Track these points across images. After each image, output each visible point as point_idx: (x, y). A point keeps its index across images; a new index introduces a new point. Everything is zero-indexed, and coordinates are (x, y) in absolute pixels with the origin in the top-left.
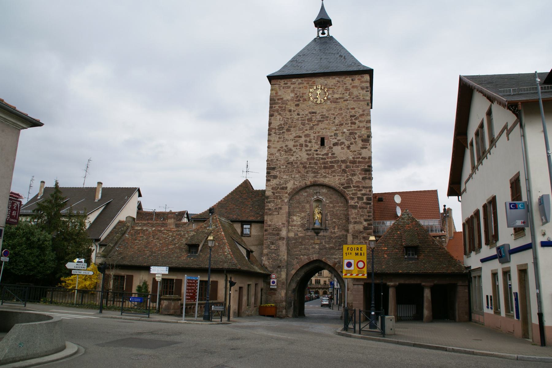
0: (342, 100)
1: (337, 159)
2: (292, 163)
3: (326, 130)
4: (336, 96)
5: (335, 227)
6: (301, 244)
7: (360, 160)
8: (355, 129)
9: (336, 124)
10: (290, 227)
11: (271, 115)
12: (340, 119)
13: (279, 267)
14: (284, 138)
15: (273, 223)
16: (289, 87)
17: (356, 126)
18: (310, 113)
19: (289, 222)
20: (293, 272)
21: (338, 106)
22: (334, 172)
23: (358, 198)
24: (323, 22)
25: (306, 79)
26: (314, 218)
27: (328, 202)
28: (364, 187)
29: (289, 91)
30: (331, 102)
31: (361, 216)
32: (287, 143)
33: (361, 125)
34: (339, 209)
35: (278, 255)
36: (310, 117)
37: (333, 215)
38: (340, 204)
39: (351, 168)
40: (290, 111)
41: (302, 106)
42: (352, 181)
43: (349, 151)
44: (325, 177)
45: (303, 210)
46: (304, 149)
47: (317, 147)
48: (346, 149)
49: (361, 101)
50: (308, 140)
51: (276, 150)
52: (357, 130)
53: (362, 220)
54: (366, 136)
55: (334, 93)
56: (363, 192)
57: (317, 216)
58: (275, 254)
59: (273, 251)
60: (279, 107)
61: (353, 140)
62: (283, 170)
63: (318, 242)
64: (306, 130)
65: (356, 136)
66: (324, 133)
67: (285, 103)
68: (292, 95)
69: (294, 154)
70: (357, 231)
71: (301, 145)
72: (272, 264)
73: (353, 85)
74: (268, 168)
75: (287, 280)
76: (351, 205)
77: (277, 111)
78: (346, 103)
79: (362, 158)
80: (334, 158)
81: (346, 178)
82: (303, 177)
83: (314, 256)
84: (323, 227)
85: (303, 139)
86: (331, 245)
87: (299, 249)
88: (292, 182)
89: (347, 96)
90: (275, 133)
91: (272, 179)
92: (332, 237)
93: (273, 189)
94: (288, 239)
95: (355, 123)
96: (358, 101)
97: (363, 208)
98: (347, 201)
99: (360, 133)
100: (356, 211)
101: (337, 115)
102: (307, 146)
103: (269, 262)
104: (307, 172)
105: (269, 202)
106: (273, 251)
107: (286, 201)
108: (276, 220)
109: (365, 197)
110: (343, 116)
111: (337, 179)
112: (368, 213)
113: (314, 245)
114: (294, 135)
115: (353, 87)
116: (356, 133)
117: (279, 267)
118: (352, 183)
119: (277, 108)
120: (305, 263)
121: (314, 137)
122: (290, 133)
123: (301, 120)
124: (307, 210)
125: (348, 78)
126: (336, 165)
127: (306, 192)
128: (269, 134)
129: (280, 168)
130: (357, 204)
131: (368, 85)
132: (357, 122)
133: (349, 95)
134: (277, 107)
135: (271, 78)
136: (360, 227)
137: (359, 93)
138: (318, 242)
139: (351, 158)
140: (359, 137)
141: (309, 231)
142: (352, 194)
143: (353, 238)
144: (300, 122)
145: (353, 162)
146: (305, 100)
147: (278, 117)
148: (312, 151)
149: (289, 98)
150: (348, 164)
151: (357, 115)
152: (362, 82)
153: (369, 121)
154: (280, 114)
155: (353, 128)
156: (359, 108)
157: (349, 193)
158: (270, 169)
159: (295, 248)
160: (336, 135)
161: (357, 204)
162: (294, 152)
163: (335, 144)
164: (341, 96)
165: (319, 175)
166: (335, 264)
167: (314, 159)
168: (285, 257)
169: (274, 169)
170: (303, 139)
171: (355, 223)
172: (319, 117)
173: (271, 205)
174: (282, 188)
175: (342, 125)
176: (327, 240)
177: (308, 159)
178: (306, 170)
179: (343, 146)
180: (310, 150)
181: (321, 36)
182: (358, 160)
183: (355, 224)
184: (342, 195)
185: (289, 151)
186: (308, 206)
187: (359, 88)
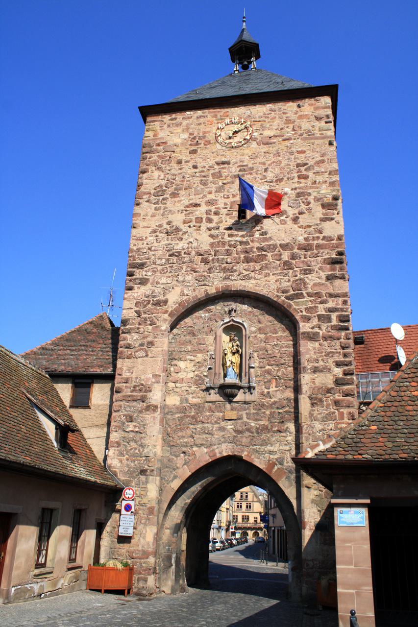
0: (280, 139)
1: (271, 242)
2: (179, 253)
4: (268, 133)
5: (269, 381)
6: (195, 420)
7: (321, 242)
8: (306, 187)
9: (268, 179)
10: (171, 385)
12: (277, 171)
13: (143, 472)
14: (165, 208)
15: (134, 375)
17: (309, 182)
18: (218, 164)
19: (169, 374)
20: (176, 484)
21: (273, 149)
22: (267, 267)
23: (320, 317)
27: (253, 329)
28: (331, 295)
29: (179, 130)
30: (258, 144)
31: (327, 354)
32: (171, 217)
33: (319, 179)
35: (142, 446)
36: (217, 170)
37: (267, 357)
38: (280, 334)
39: (303, 259)
40: (179, 162)
42: (305, 283)
43: (296, 226)
44: (247, 278)
45: (200, 348)
46: (204, 225)
48: (289, 222)
49: (317, 138)
50: (213, 210)
51: (149, 230)
52: (311, 188)
53: (330, 362)
54: (330, 197)
55: (263, 128)
56: (331, 304)
58: (135, 442)
59: (131, 435)
60: (159, 156)
61: (303, 207)
62: (160, 268)
64: (210, 193)
65: (311, 199)
68: (186, 136)
69: (185, 237)
70: (319, 389)
71: (199, 220)
72: (128, 466)
73: (300, 113)
75: (159, 502)
76: (303, 333)
77: (155, 164)
78: (287, 143)
79: (324, 238)
80: (266, 240)
81: (292, 279)
83: (224, 446)
84: (244, 383)
85: (204, 208)
87: (189, 432)
88: (178, 290)
89: (289, 132)
90: (148, 201)
91: (136, 286)
92: (263, 405)
93: (136, 305)
94: (166, 411)
95: (306, 177)
96: (312, 139)
97: (331, 338)
99: (318, 193)
100: (317, 344)
101: (269, 165)
102: (210, 221)
103: (121, 461)
104: (210, 270)
105: (129, 332)
106: (131, 435)
107: (163, 328)
108: (141, 367)
109: (334, 316)
110: (283, 165)
111: (273, 282)
112: (343, 348)
113: (223, 424)
114: (186, 203)
115: (301, 117)
116: (310, 194)
117: (143, 472)
118: (306, 288)
119: (156, 158)
120: (202, 464)
121: (226, 204)
122: (177, 199)
123: (200, 176)
124: (210, 348)
125: (291, 104)
126: (269, 255)
127: (209, 311)
129: (154, 263)
130: (317, 330)
131: (329, 112)
132: (310, 174)
133: (293, 130)
136: (327, 380)
137: (313, 127)
138: (233, 415)
139: (301, 239)
140: (317, 200)
141: (212, 391)
142: (306, 309)
143: (313, 404)
144: (198, 180)
145: (306, 248)
147: (156, 174)
148: (222, 230)
149: (178, 141)
150: (296, 250)
151: (311, 162)
152: (317, 108)
154: (159, 169)
155: (302, 185)
156: (313, 151)
157: (298, 308)
159: (181, 430)
161: (317, 330)
162: (185, 233)
164: (278, 133)
165: (235, 274)
166: (272, 465)
167: (224, 244)
168: (158, 450)
169: (141, 266)
170: (204, 208)
171: (316, 370)
174: (158, 304)
175: (281, 180)
176: (253, 411)
177: (212, 245)
178: (207, 267)
179: (283, 218)
180: (218, 228)
182: (315, 242)
183: (315, 372)
185: (173, 232)
187: (313, 118)
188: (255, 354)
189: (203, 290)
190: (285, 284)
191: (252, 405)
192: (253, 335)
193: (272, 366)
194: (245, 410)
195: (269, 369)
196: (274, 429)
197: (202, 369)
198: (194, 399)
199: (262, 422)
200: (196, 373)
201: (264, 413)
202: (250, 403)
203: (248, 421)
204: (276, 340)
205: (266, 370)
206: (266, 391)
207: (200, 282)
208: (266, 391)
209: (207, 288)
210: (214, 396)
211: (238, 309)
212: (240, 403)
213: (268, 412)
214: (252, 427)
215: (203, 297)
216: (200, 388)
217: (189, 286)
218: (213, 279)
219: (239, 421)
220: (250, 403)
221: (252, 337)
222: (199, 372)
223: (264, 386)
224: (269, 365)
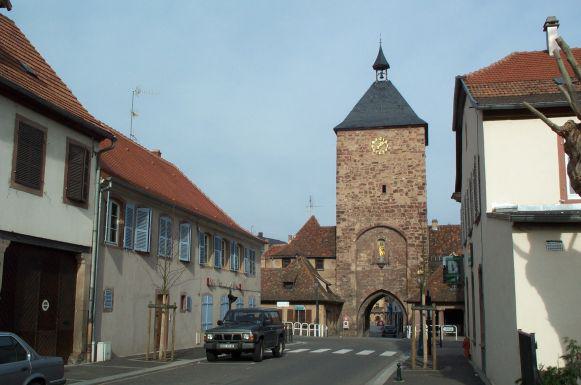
3: (388, 178)
4: (395, 148)
11: (339, 165)
16: (353, 139)
20: (362, 300)
24: (381, 65)
25: (369, 131)
34: (401, 245)
41: (366, 156)
44: (387, 220)
47: (380, 193)
57: (381, 253)
66: (387, 181)
67: (350, 153)
71: (366, 192)
74: (338, 212)
82: (369, 220)
85: (367, 186)
94: (357, 273)
98: (406, 240)
128: (338, 182)
131: (423, 137)
134: (343, 157)
135: (336, 130)
139: (409, 203)
145: (411, 207)
146: (368, 151)
153: (424, 171)
157: (407, 233)
158: (339, 213)
160: (396, 183)
163: (395, 191)
169: (343, 212)
170: (367, 186)
172: (380, 167)
173: (342, 244)
181: (380, 80)
184: (401, 234)
185: (355, 197)
186: (373, 244)
190: (402, 223)
210: (376, 267)
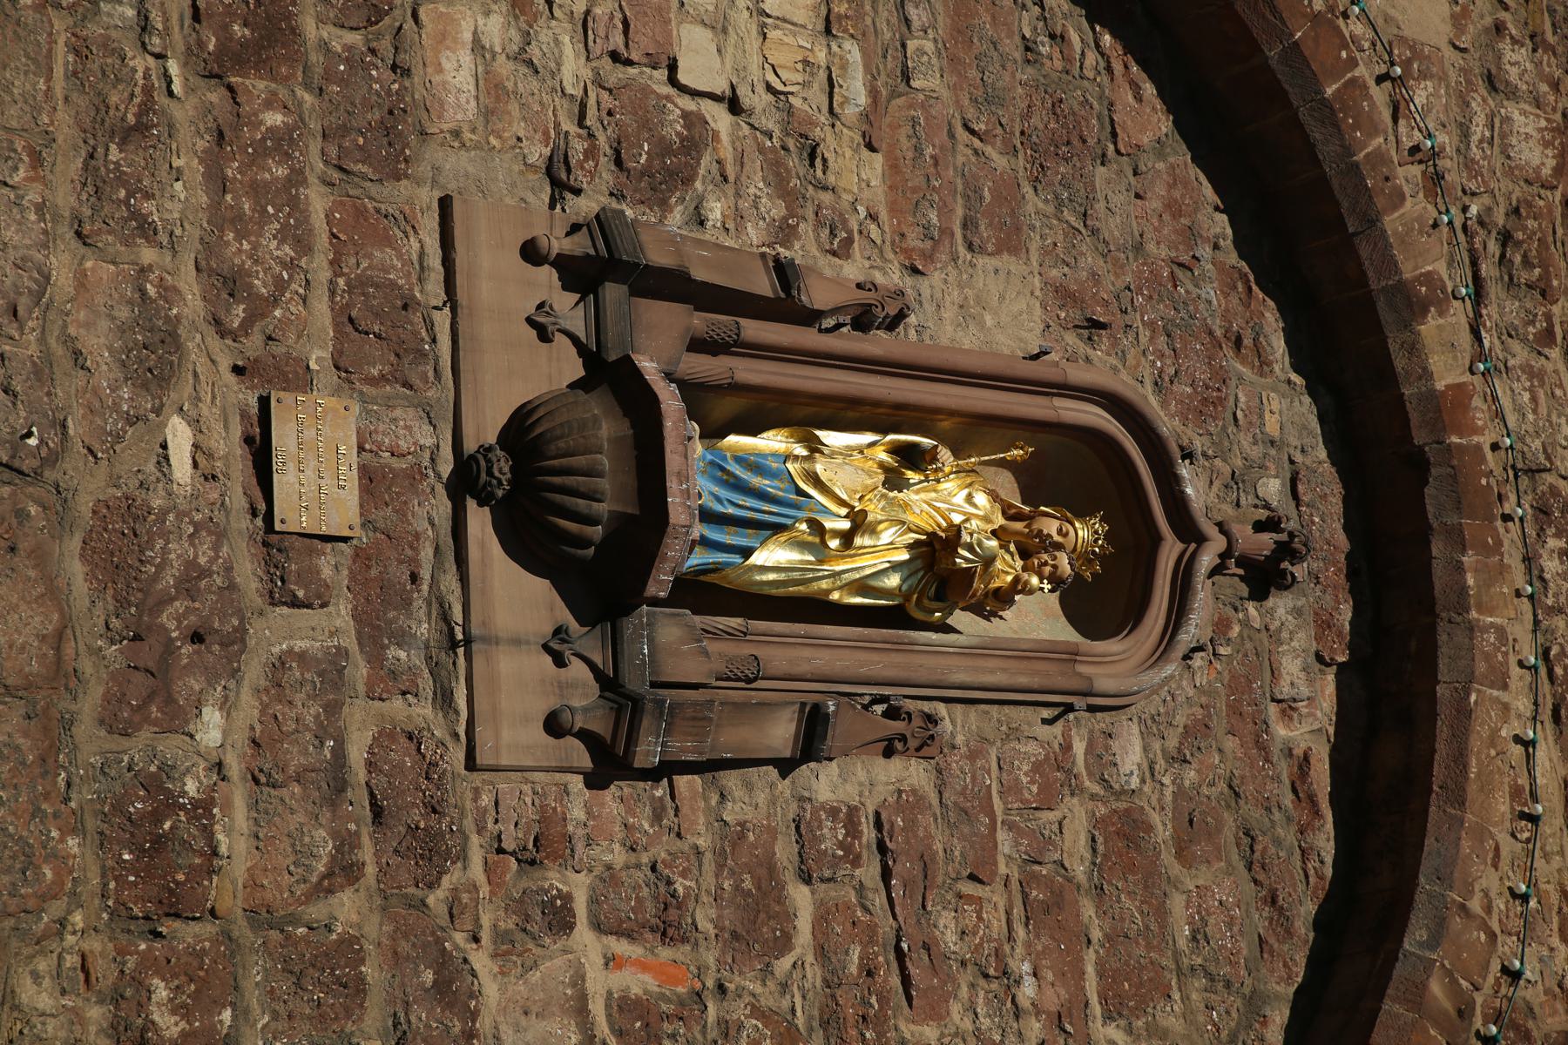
5: (668, 925)
26: (807, 415)
27: (1130, 755)
63: (319, 482)
86: (233, 836)
92: (431, 852)
138: (319, 482)
188: (913, 773)
189: (1441, 268)
191: (424, 711)
192: (1079, 748)
193: (821, 952)
194: (375, 631)
195: (789, 917)
196: (161, 992)
197: (756, 185)
198: (466, 58)
199: (242, 845)
200: (720, 118)
201: (345, 871)
202: (444, 699)
203: (254, 671)
204: (1052, 1001)
205: (781, 886)
206: (579, 887)
207: (1494, 247)
208: (579, 887)
209: (1459, 314)
211: (1281, 604)
212: (450, 582)
213: (347, 909)
214: (179, 720)
215: (1392, 265)
216: (578, 147)
217: (1465, 134)
218: (1529, 370)
219: (249, 575)
220: (444, 699)
221: (1067, 747)
222: (727, 153)
223: (618, 856)
224: (822, 920)
